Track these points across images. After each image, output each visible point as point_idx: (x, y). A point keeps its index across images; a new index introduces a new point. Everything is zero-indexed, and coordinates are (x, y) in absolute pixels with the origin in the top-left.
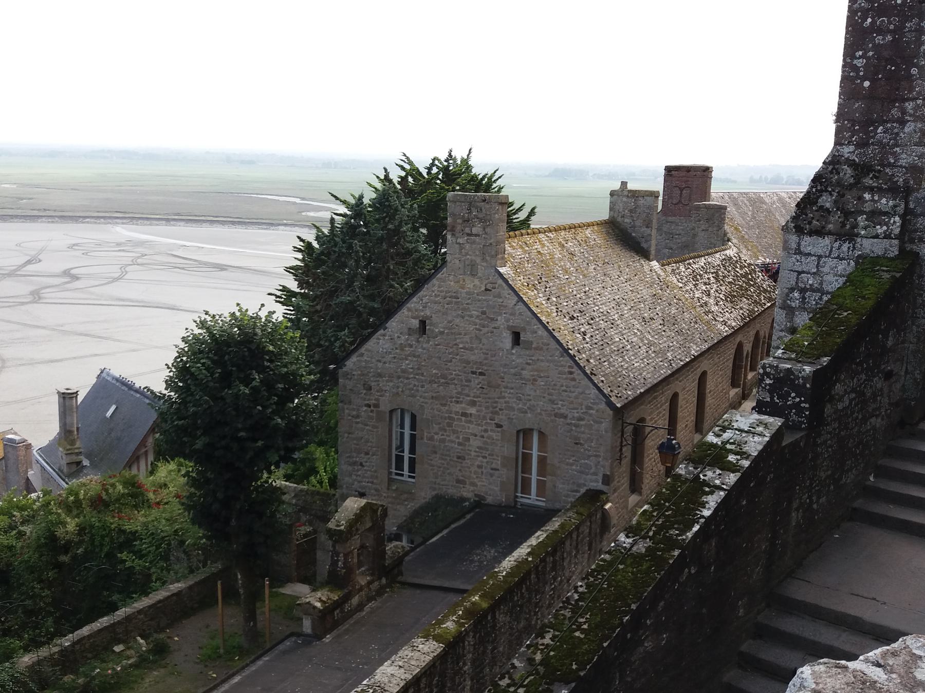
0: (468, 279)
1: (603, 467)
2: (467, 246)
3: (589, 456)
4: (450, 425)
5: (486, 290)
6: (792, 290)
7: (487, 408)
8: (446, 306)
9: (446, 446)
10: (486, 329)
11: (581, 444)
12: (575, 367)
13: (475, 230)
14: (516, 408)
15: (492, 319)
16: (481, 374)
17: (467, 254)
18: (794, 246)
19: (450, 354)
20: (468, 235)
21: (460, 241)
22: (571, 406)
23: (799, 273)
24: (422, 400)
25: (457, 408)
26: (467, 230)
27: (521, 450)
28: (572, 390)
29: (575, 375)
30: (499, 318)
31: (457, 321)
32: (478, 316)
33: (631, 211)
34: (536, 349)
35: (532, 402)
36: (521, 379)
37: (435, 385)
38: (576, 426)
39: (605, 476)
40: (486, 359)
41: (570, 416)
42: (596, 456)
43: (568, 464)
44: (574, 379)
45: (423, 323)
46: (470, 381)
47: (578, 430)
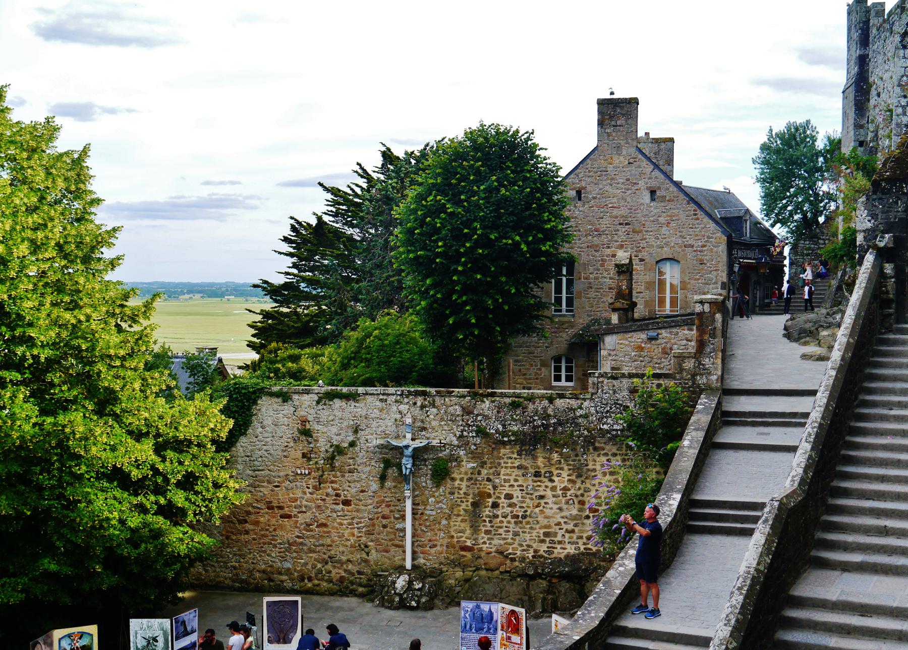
0: (615, 157)
1: (722, 277)
2: (614, 134)
3: (711, 271)
4: (602, 265)
5: (629, 163)
6: (902, 76)
7: (632, 248)
8: (598, 178)
9: (599, 282)
10: (630, 192)
11: (704, 263)
12: (699, 211)
13: (619, 123)
14: (655, 245)
15: (635, 184)
16: (627, 224)
17: (614, 140)
18: (902, 55)
19: (601, 212)
20: (614, 126)
21: (608, 131)
22: (697, 238)
23: (906, 68)
24: (579, 250)
25: (608, 251)
26: (613, 123)
27: (657, 277)
28: (697, 226)
29: (699, 216)
30: (640, 182)
31: (607, 188)
32: (623, 183)
33: (655, 154)
34: (669, 201)
35: (667, 240)
36: (658, 224)
37: (590, 238)
38: (701, 251)
39: (723, 283)
40: (630, 213)
41: (696, 245)
42: (716, 270)
43: (695, 279)
44: (698, 219)
45: (579, 193)
46: (618, 230)
47: (702, 254)
